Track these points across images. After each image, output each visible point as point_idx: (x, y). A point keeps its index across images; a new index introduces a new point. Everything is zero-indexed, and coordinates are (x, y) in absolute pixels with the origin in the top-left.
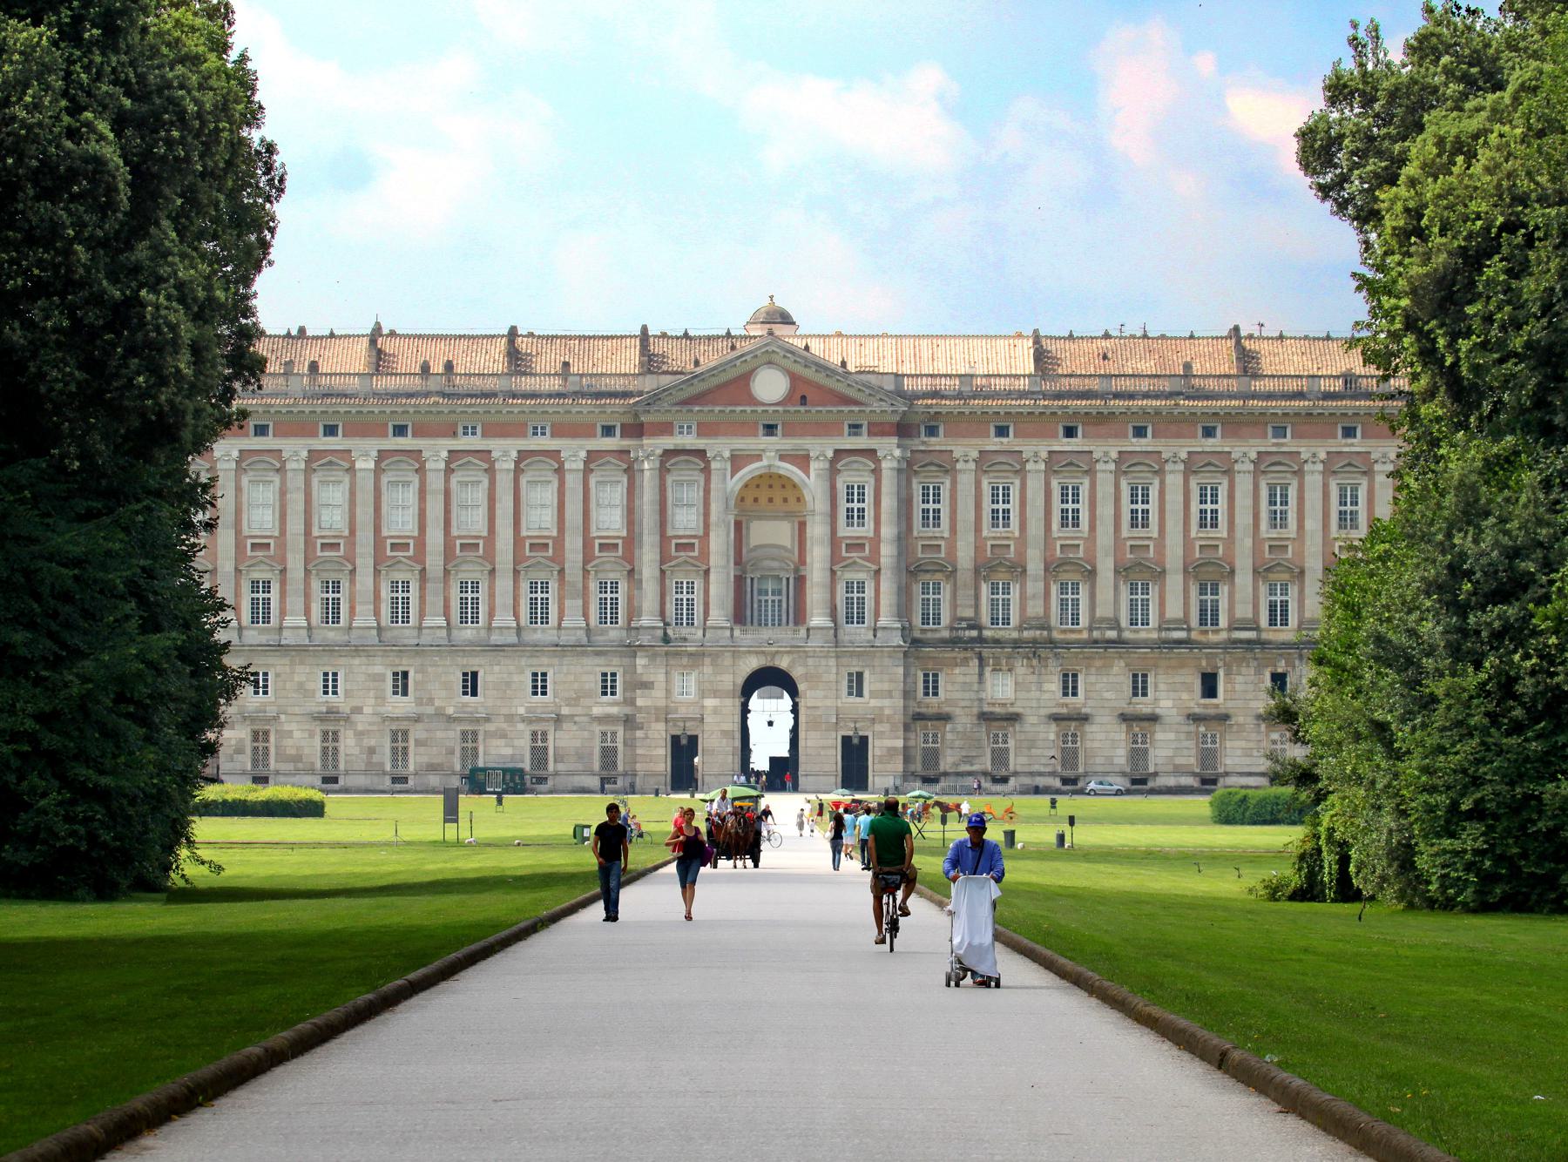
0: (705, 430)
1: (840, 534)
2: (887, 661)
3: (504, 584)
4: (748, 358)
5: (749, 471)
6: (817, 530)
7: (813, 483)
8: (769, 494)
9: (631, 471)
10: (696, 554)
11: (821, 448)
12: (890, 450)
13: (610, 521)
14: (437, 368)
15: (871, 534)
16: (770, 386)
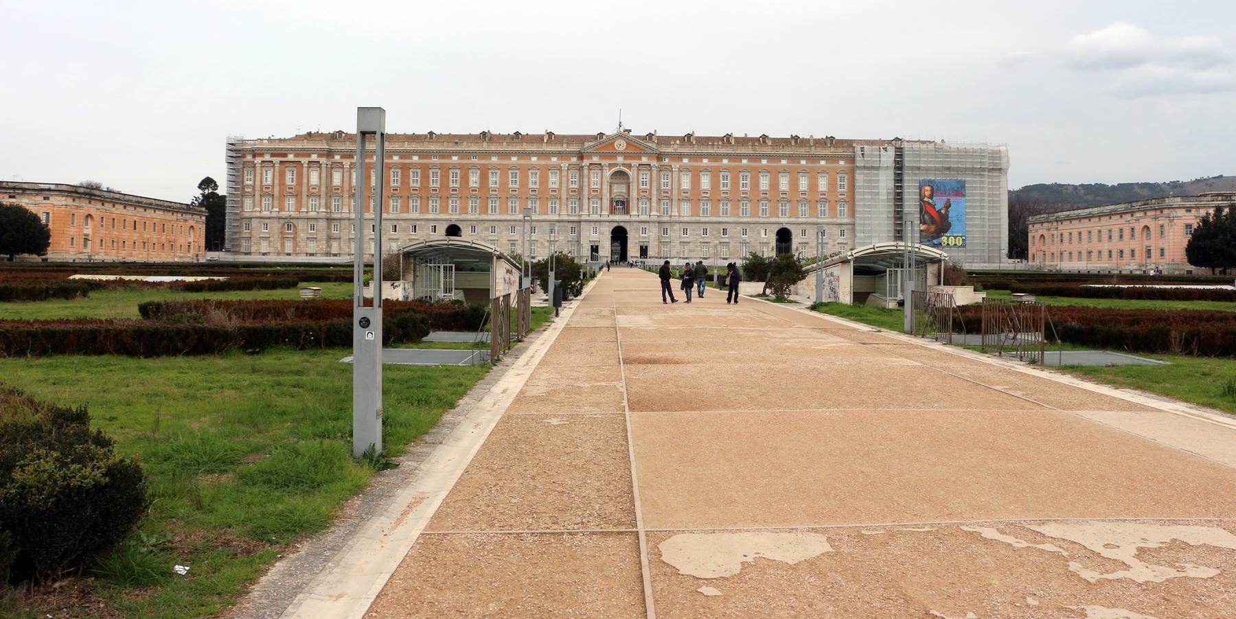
7: (632, 173)
11: (635, 163)
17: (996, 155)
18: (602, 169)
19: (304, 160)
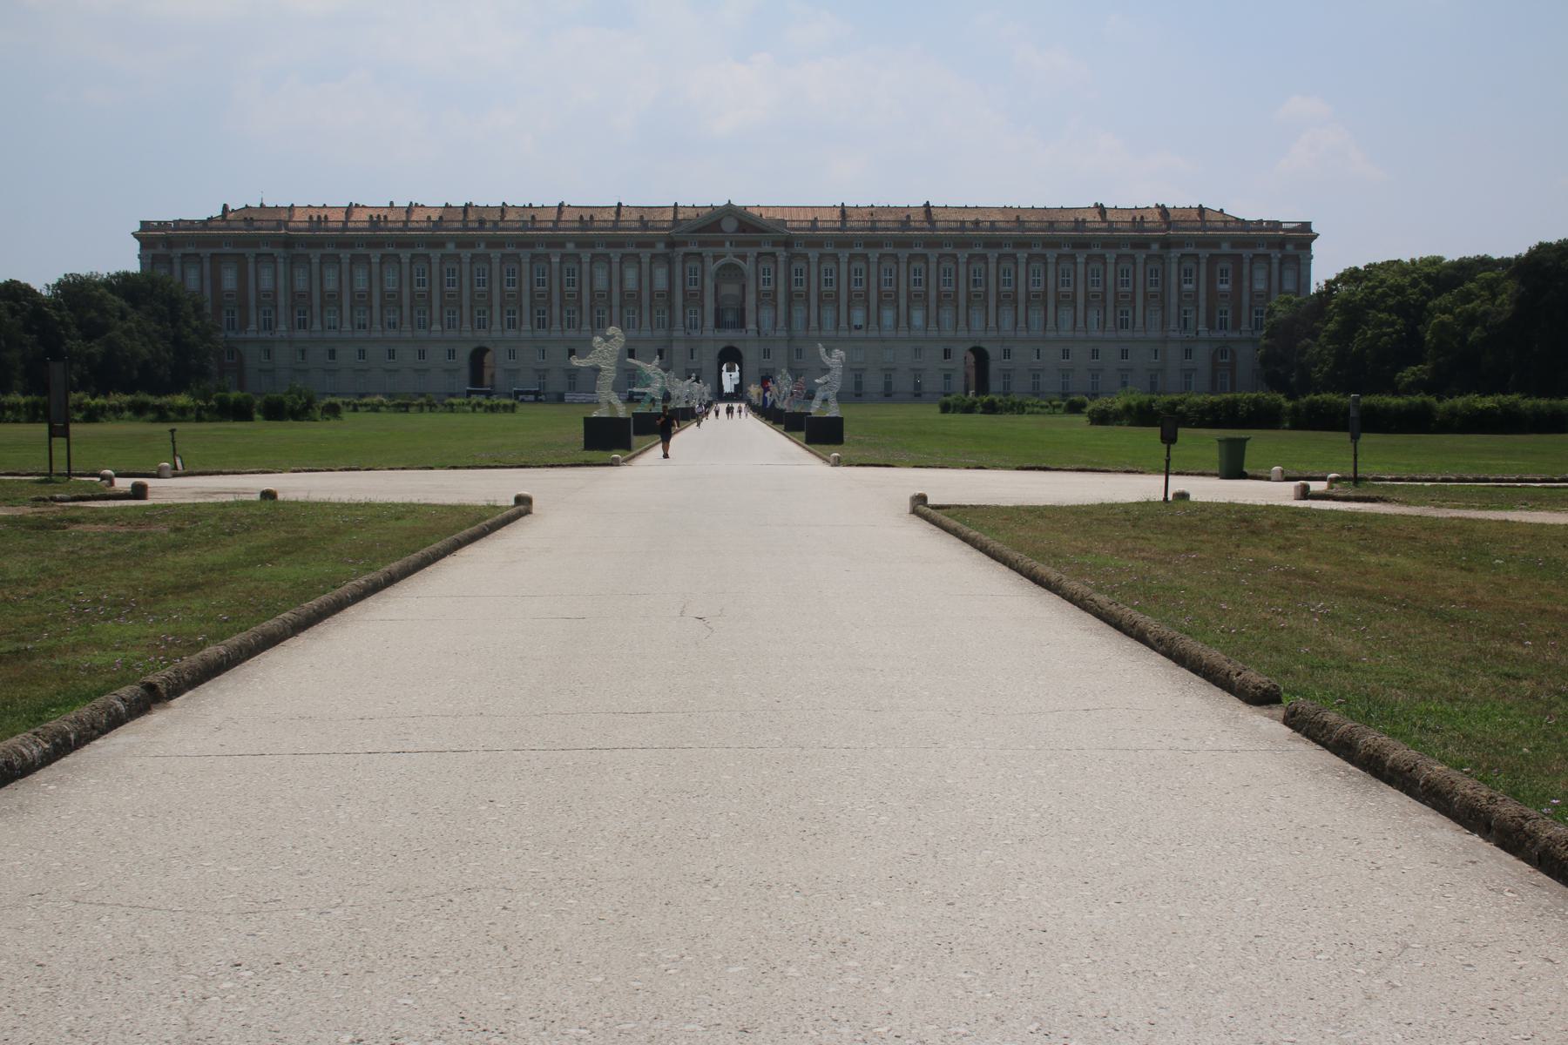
0: (703, 244)
3: (616, 311)
5: (721, 262)
6: (751, 287)
7: (748, 267)
8: (730, 272)
9: (669, 261)
11: (752, 252)
12: (781, 253)
13: (661, 282)
14: (587, 218)
16: (729, 225)
17: (1306, 226)
18: (702, 262)
19: (250, 252)
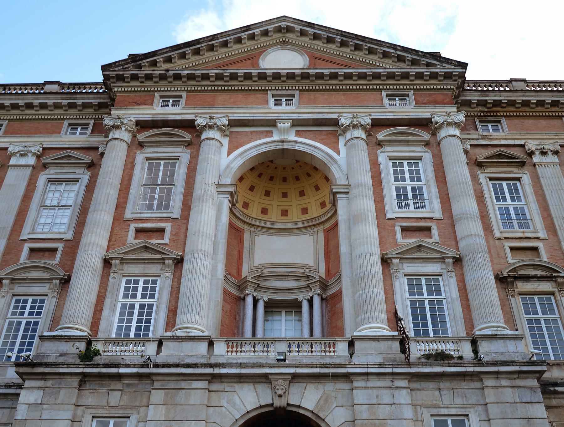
1: (390, 215)
2: (509, 395)
4: (257, 31)
5: (256, 146)
7: (346, 160)
10: (166, 240)
15: (438, 214)
18: (194, 145)
